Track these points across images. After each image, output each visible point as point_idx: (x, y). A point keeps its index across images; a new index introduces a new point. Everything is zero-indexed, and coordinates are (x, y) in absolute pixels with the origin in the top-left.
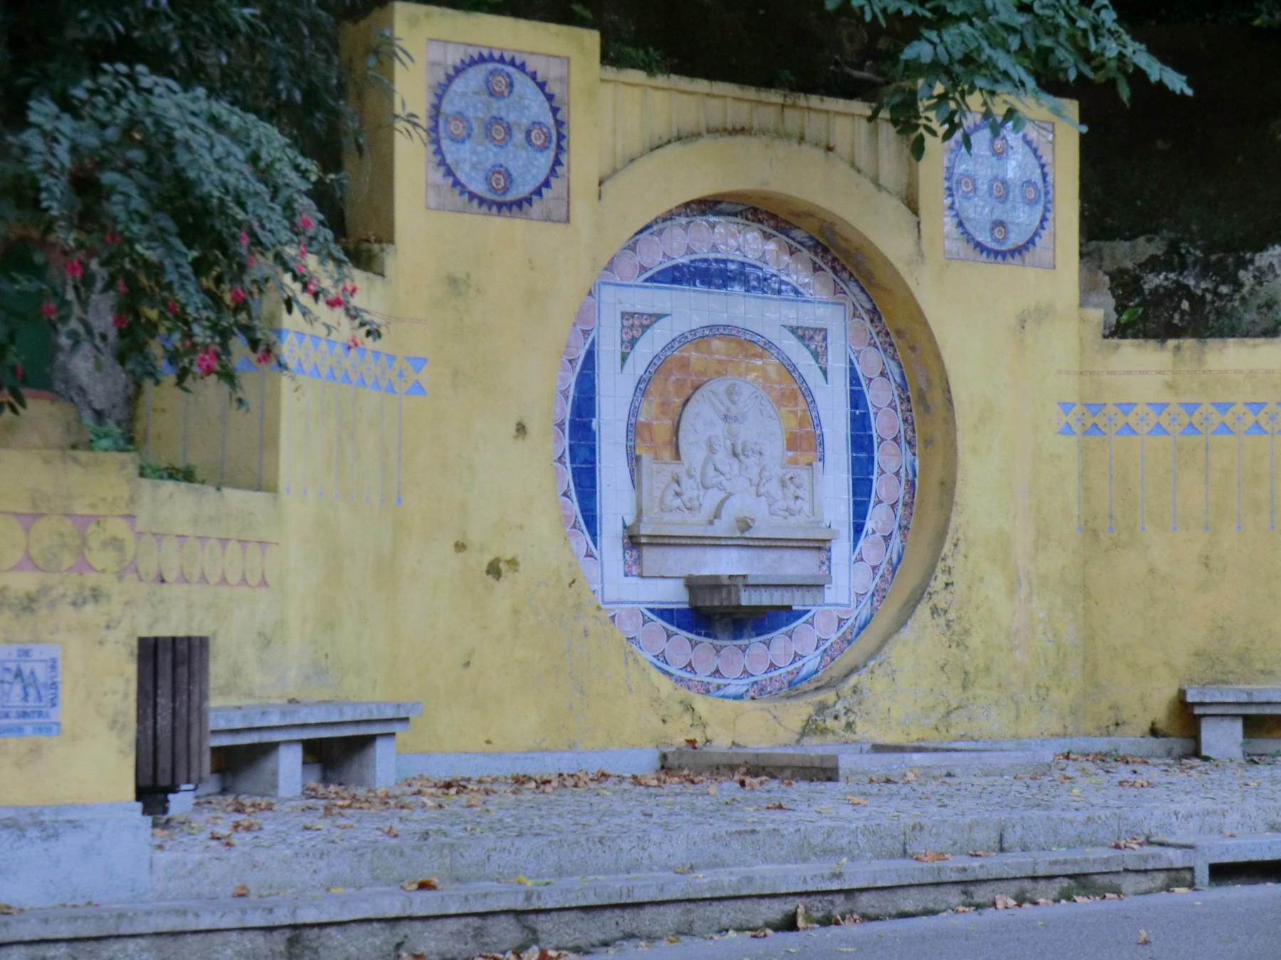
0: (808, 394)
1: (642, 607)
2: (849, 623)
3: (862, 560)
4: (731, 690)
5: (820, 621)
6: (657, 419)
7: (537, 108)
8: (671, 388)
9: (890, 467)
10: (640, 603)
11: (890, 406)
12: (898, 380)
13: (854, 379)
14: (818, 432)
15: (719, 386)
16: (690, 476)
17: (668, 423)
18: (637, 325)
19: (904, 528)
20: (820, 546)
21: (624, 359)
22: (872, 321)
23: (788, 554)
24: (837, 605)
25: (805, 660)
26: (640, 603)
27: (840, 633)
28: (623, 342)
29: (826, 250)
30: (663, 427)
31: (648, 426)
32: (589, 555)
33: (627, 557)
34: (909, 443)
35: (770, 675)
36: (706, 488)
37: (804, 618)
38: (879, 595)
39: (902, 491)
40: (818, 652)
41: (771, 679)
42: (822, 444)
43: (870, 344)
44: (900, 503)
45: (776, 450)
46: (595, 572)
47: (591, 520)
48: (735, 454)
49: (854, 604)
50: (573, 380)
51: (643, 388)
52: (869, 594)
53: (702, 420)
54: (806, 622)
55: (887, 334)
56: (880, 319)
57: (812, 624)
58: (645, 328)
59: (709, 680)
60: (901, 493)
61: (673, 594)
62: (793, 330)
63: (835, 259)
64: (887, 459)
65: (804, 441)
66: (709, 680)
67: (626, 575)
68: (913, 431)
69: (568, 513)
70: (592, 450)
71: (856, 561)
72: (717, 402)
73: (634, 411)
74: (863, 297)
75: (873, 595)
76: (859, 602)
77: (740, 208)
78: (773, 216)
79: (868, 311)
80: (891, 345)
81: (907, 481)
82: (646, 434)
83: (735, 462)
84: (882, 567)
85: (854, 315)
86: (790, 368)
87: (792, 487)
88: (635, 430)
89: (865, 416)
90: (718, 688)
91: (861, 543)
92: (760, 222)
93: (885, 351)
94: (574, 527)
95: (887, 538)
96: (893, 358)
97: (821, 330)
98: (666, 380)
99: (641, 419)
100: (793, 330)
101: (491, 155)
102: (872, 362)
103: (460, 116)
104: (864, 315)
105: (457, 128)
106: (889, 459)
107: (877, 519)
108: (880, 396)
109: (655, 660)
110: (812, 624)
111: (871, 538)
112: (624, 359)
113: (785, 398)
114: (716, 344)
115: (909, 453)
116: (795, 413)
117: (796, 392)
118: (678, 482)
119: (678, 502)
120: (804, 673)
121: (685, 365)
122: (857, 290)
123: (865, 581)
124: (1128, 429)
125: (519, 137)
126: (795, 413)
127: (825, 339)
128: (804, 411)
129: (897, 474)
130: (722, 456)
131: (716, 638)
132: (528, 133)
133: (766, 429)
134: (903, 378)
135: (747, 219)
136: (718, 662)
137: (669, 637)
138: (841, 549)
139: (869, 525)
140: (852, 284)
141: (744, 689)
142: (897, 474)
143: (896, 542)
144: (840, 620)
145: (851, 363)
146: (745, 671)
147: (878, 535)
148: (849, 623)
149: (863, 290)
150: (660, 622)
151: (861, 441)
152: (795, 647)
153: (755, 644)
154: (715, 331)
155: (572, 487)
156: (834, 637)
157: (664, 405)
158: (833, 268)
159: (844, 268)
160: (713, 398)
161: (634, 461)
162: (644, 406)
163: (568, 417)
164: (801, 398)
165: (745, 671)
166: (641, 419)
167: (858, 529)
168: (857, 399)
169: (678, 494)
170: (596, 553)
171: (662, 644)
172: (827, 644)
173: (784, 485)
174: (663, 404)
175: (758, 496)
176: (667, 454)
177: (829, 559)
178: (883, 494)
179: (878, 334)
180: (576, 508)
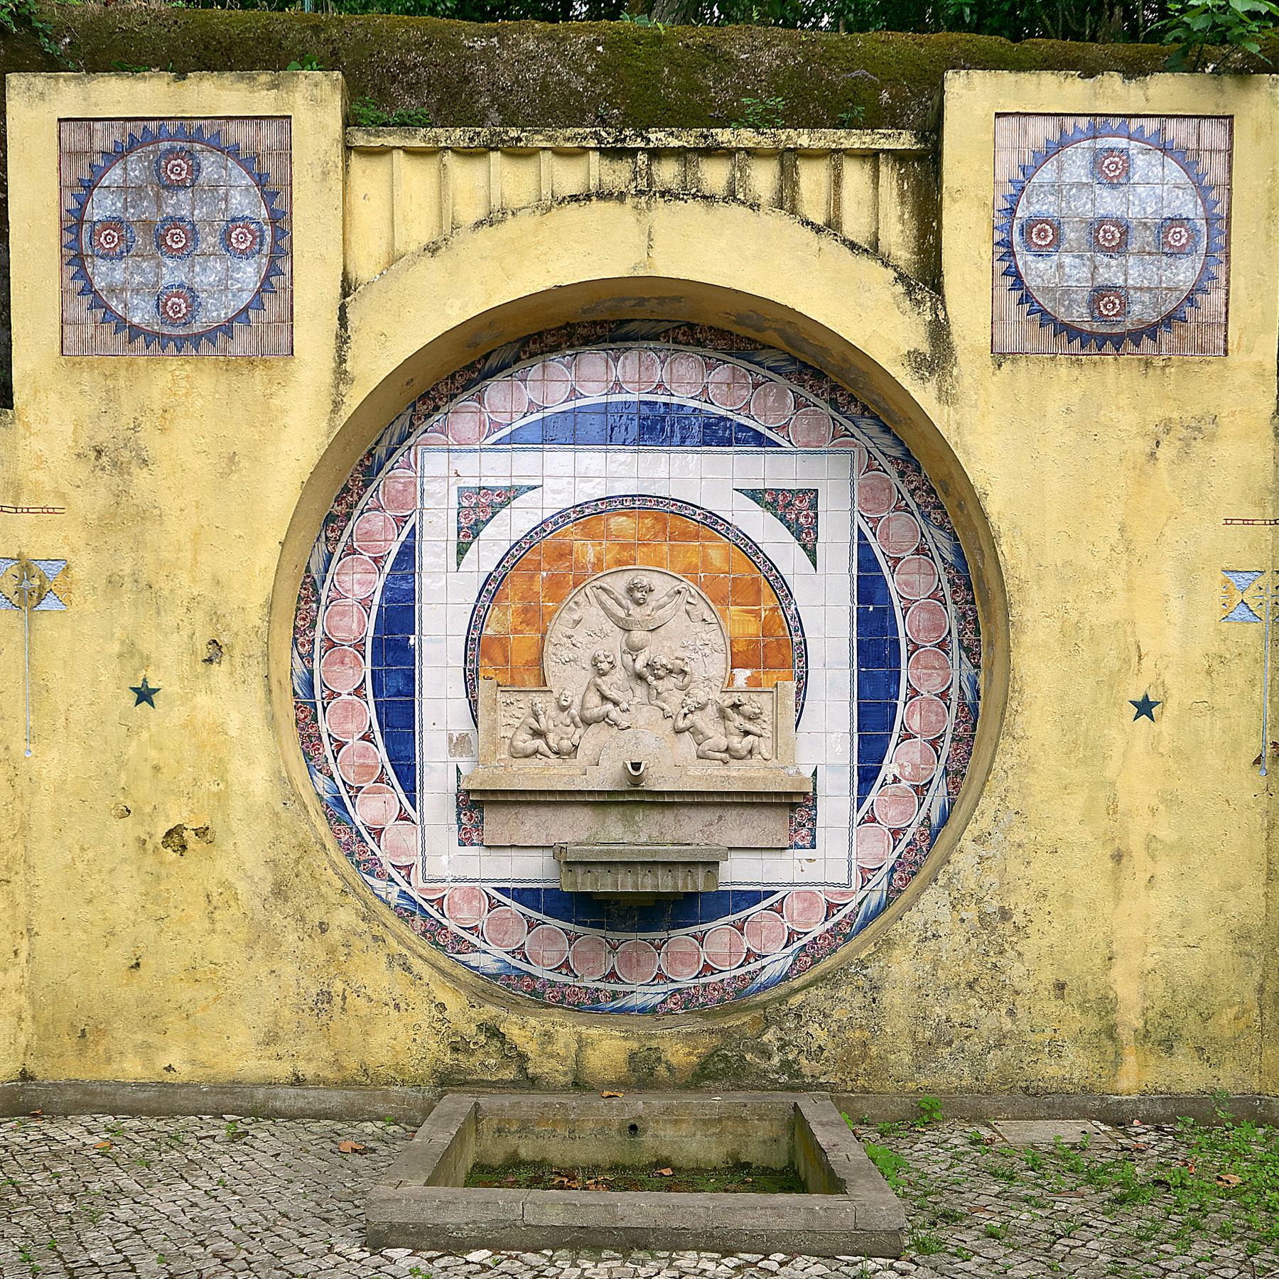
1: (488, 887)
2: (846, 910)
3: (874, 820)
4: (637, 1000)
5: (794, 906)
6: (516, 631)
7: (243, 200)
8: (538, 587)
9: (930, 686)
10: (483, 881)
11: (933, 596)
12: (950, 558)
13: (866, 560)
14: (796, 639)
15: (618, 584)
16: (564, 709)
17: (532, 635)
19: (955, 776)
20: (794, 804)
21: (462, 551)
22: (902, 474)
23: (731, 815)
24: (826, 884)
25: (764, 962)
26: (483, 881)
27: (829, 925)
28: (459, 530)
29: (819, 375)
31: (501, 641)
32: (404, 817)
33: (464, 819)
34: (967, 650)
35: (702, 980)
36: (587, 723)
37: (765, 903)
39: (951, 720)
40: (789, 950)
41: (705, 986)
42: (804, 655)
43: (897, 509)
44: (948, 737)
45: (710, 666)
46: (413, 840)
47: (406, 771)
48: (640, 677)
49: (856, 883)
50: (380, 584)
51: (492, 588)
52: (885, 869)
53: (582, 634)
54: (771, 908)
55: (931, 491)
56: (918, 469)
57: (780, 912)
58: (495, 510)
59: (601, 985)
61: (532, 868)
62: (754, 495)
63: (834, 388)
65: (775, 651)
66: (601, 985)
67: (462, 843)
68: (978, 632)
69: (370, 762)
70: (410, 678)
71: (863, 821)
72: (610, 603)
73: (477, 620)
74: (888, 440)
75: (893, 870)
76: (865, 881)
77: (662, 327)
78: (722, 334)
79: (894, 460)
80: (939, 507)
81: (962, 705)
82: (497, 653)
83: (640, 690)
84: (910, 831)
85: (870, 468)
86: (750, 549)
87: (738, 720)
88: (476, 646)
89: (886, 613)
90: (615, 996)
91: (872, 796)
92: (699, 343)
93: (925, 516)
94: (380, 780)
95: (921, 790)
96: (941, 527)
97: (805, 492)
98: (532, 577)
99: (488, 632)
100: (754, 495)
102: (898, 535)
104: (887, 466)
105: (108, 240)
106: (922, 678)
107: (899, 761)
109: (508, 958)
110: (780, 912)
111: (891, 789)
112: (462, 551)
113: (724, 593)
114: (619, 523)
115: (967, 665)
116: (757, 614)
118: (536, 716)
119: (539, 743)
120: (763, 978)
121: (563, 554)
122: (875, 431)
123: (877, 849)
126: (757, 614)
127: (814, 506)
128: (774, 610)
129: (944, 695)
130: (615, 683)
131: (612, 928)
132: (226, 236)
134: (959, 553)
135: (676, 341)
136: (613, 961)
137: (531, 927)
139: (888, 769)
140: (864, 423)
141: (660, 998)
142: (944, 695)
143: (937, 797)
144: (830, 906)
145: (861, 535)
146: (660, 975)
147: (904, 784)
148: (846, 910)
149: (887, 430)
150: (516, 907)
152: (747, 943)
153: (681, 938)
155: (376, 727)
156: (818, 930)
158: (834, 404)
159: (853, 399)
160: (604, 597)
162: (495, 613)
163: (371, 633)
164: (766, 590)
165: (660, 975)
166: (488, 632)
167: (867, 776)
168: (870, 586)
169: (538, 734)
170: (415, 816)
172: (805, 940)
173: (723, 716)
174: (525, 610)
175: (678, 732)
176: (530, 681)
177: (813, 820)
178: (915, 724)
179: (912, 492)
180: (382, 754)
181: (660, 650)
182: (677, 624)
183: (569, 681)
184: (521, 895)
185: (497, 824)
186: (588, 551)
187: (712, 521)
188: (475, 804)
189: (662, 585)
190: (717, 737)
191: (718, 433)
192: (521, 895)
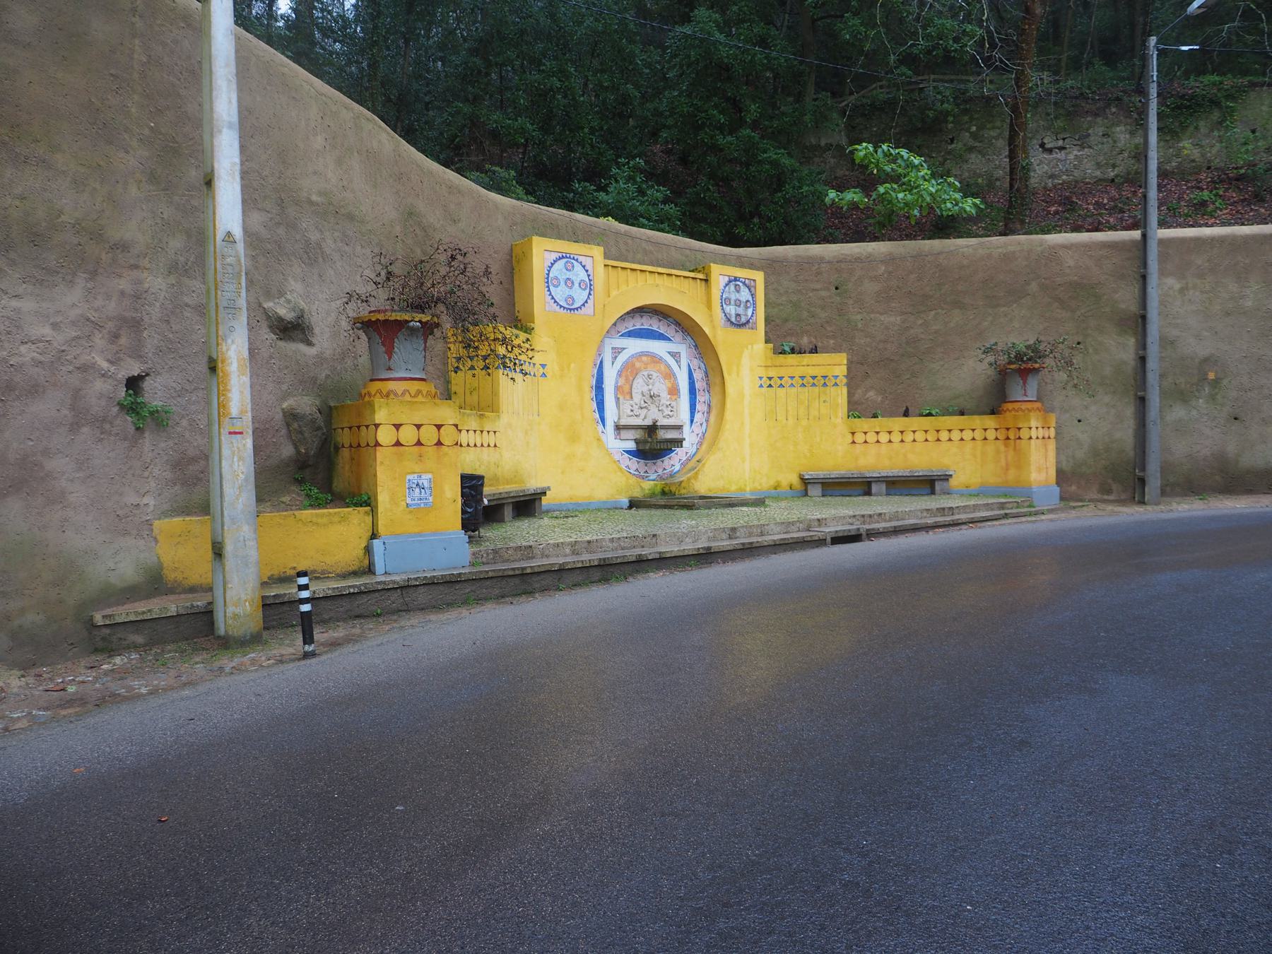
0: (674, 375)
7: (583, 276)
9: (702, 399)
18: (617, 351)
20: (679, 428)
30: (626, 388)
38: (700, 443)
47: (603, 419)
51: (620, 374)
53: (639, 386)
60: (706, 409)
61: (631, 445)
64: (701, 398)
65: (674, 391)
86: (669, 366)
88: (617, 388)
101: (568, 292)
103: (556, 278)
105: (555, 282)
108: (698, 375)
114: (644, 359)
117: (670, 375)
121: (633, 365)
124: (792, 385)
125: (576, 285)
130: (647, 398)
133: (661, 387)
138: (686, 429)
151: (692, 391)
154: (643, 354)
157: (627, 379)
161: (617, 399)
167: (692, 421)
171: (628, 462)
176: (628, 397)
181: (655, 391)
182: (657, 384)
183: (637, 398)
184: (627, 452)
185: (625, 434)
186: (638, 365)
187: (661, 359)
188: (618, 428)
189: (655, 375)
190: (667, 412)
191: (661, 337)
192: (627, 452)
